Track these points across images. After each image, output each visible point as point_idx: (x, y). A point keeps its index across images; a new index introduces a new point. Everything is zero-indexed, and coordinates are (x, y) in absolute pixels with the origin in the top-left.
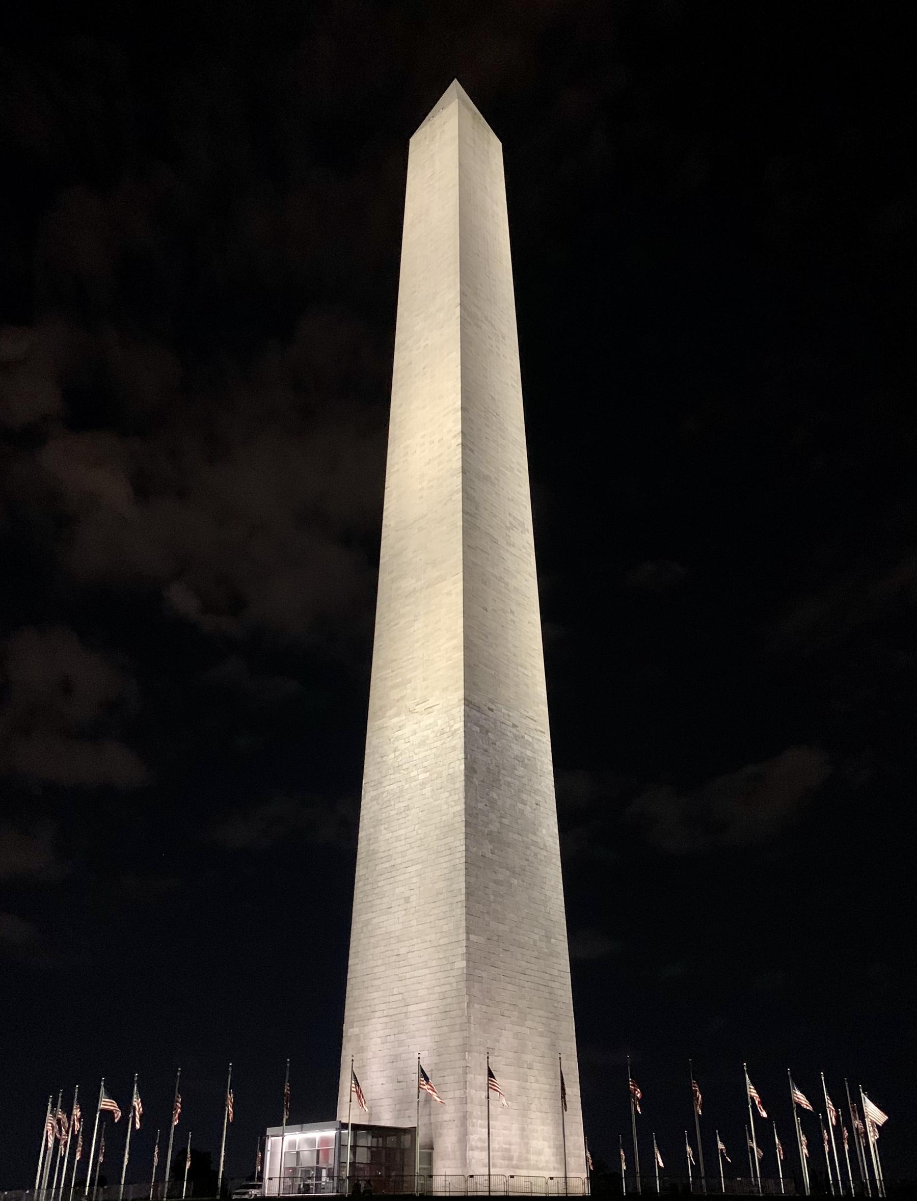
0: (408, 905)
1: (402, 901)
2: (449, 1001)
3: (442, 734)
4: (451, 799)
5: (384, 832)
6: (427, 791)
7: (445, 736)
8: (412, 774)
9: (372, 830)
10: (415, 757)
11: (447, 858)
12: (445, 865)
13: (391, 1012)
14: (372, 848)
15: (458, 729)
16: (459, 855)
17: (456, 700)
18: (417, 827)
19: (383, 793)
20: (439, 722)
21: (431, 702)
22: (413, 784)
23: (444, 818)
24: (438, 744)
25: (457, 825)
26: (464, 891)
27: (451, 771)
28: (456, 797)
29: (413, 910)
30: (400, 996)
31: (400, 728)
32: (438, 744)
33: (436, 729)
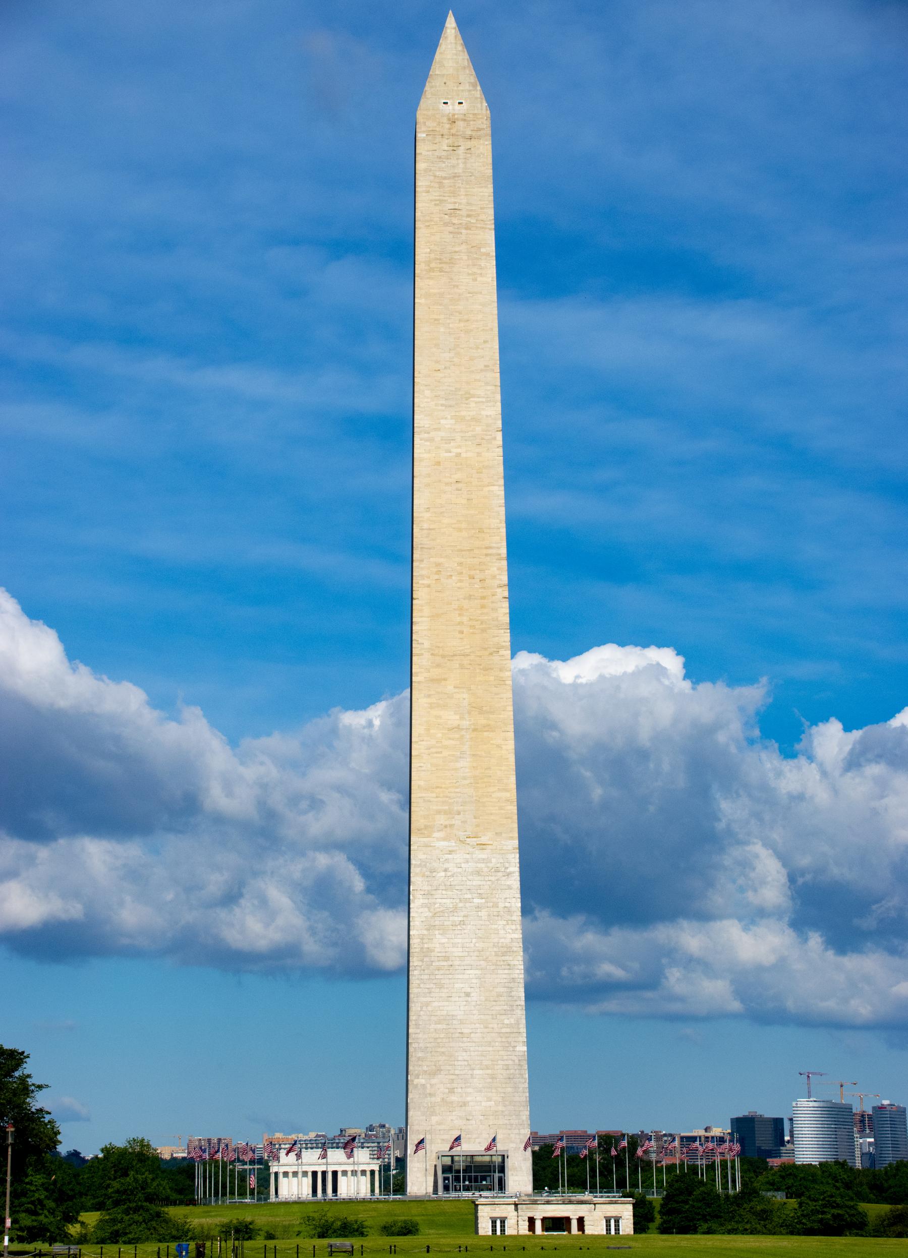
0: (469, 999)
1: (463, 995)
2: (512, 1071)
3: (497, 871)
4: (508, 927)
5: (438, 936)
6: (483, 913)
7: (500, 874)
8: (466, 896)
9: (425, 932)
10: (468, 883)
11: (506, 971)
12: (505, 976)
13: (457, 1072)
14: (426, 946)
15: (514, 873)
16: (518, 971)
17: (510, 848)
18: (474, 941)
19: (435, 904)
20: (494, 860)
21: (484, 840)
22: (468, 905)
23: (503, 940)
24: (493, 878)
25: (515, 949)
26: (523, 998)
27: (507, 905)
28: (514, 927)
29: (474, 1003)
30: (466, 1063)
31: (450, 852)
32: (493, 878)
33: (490, 865)
